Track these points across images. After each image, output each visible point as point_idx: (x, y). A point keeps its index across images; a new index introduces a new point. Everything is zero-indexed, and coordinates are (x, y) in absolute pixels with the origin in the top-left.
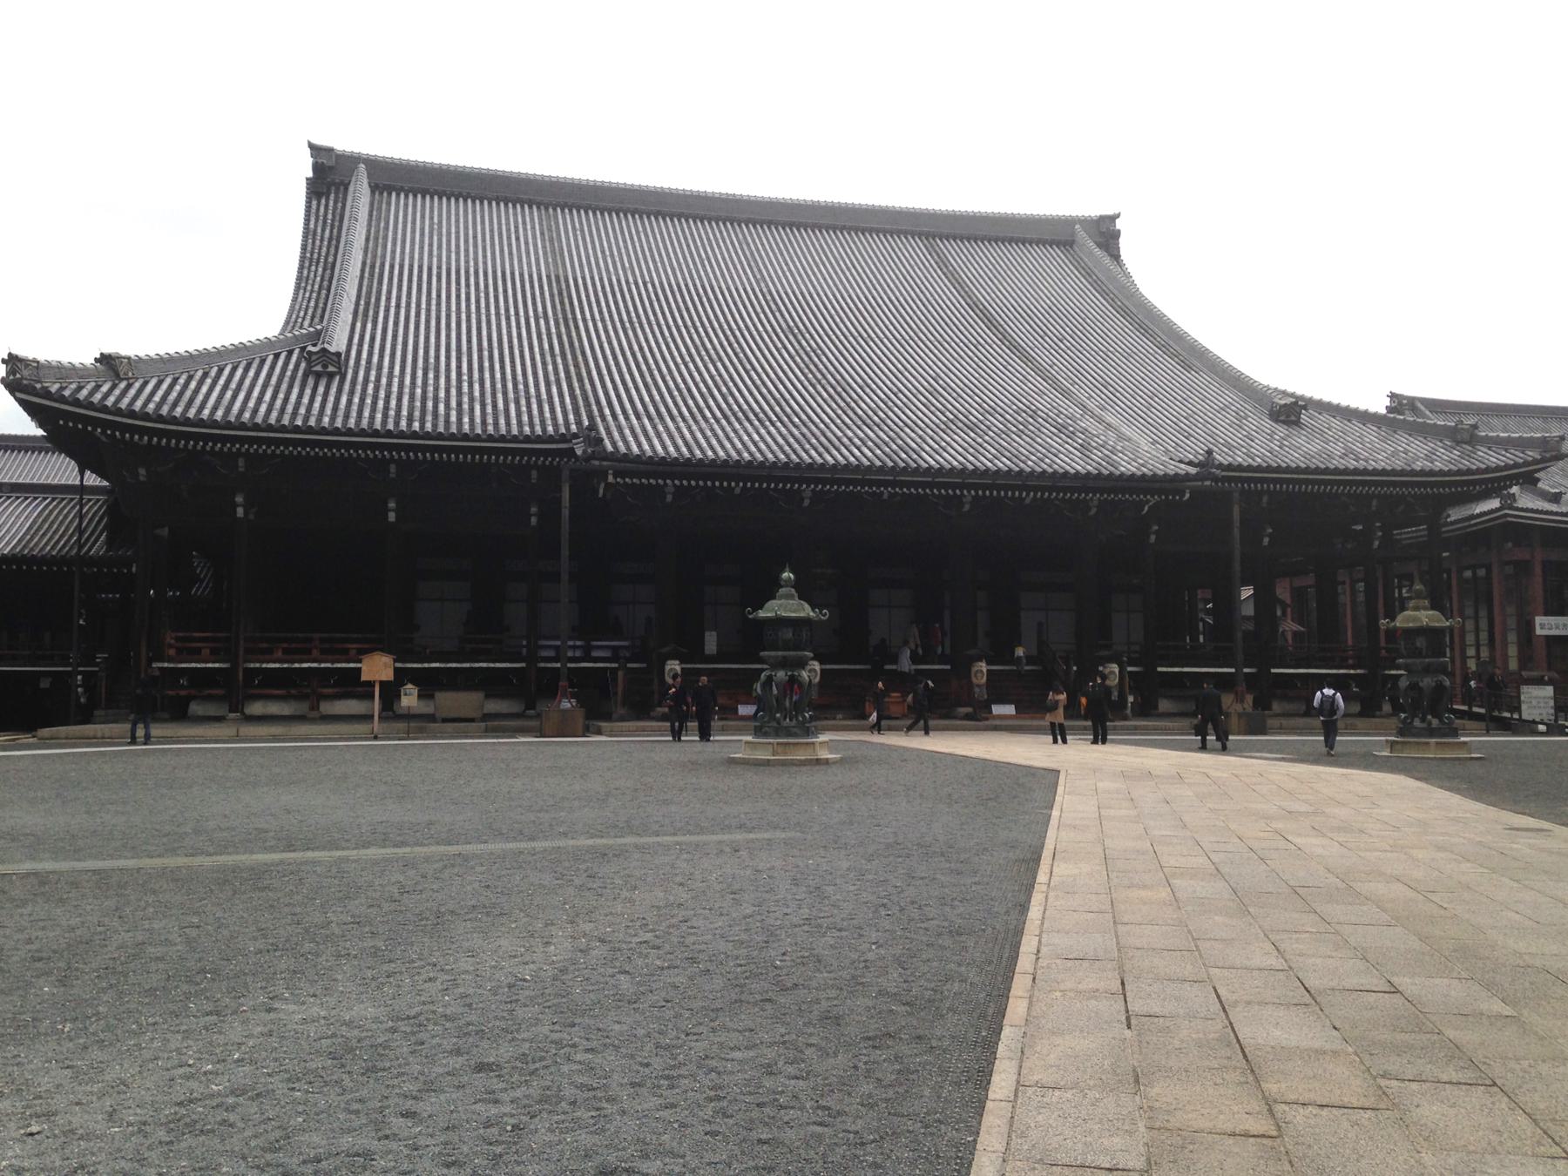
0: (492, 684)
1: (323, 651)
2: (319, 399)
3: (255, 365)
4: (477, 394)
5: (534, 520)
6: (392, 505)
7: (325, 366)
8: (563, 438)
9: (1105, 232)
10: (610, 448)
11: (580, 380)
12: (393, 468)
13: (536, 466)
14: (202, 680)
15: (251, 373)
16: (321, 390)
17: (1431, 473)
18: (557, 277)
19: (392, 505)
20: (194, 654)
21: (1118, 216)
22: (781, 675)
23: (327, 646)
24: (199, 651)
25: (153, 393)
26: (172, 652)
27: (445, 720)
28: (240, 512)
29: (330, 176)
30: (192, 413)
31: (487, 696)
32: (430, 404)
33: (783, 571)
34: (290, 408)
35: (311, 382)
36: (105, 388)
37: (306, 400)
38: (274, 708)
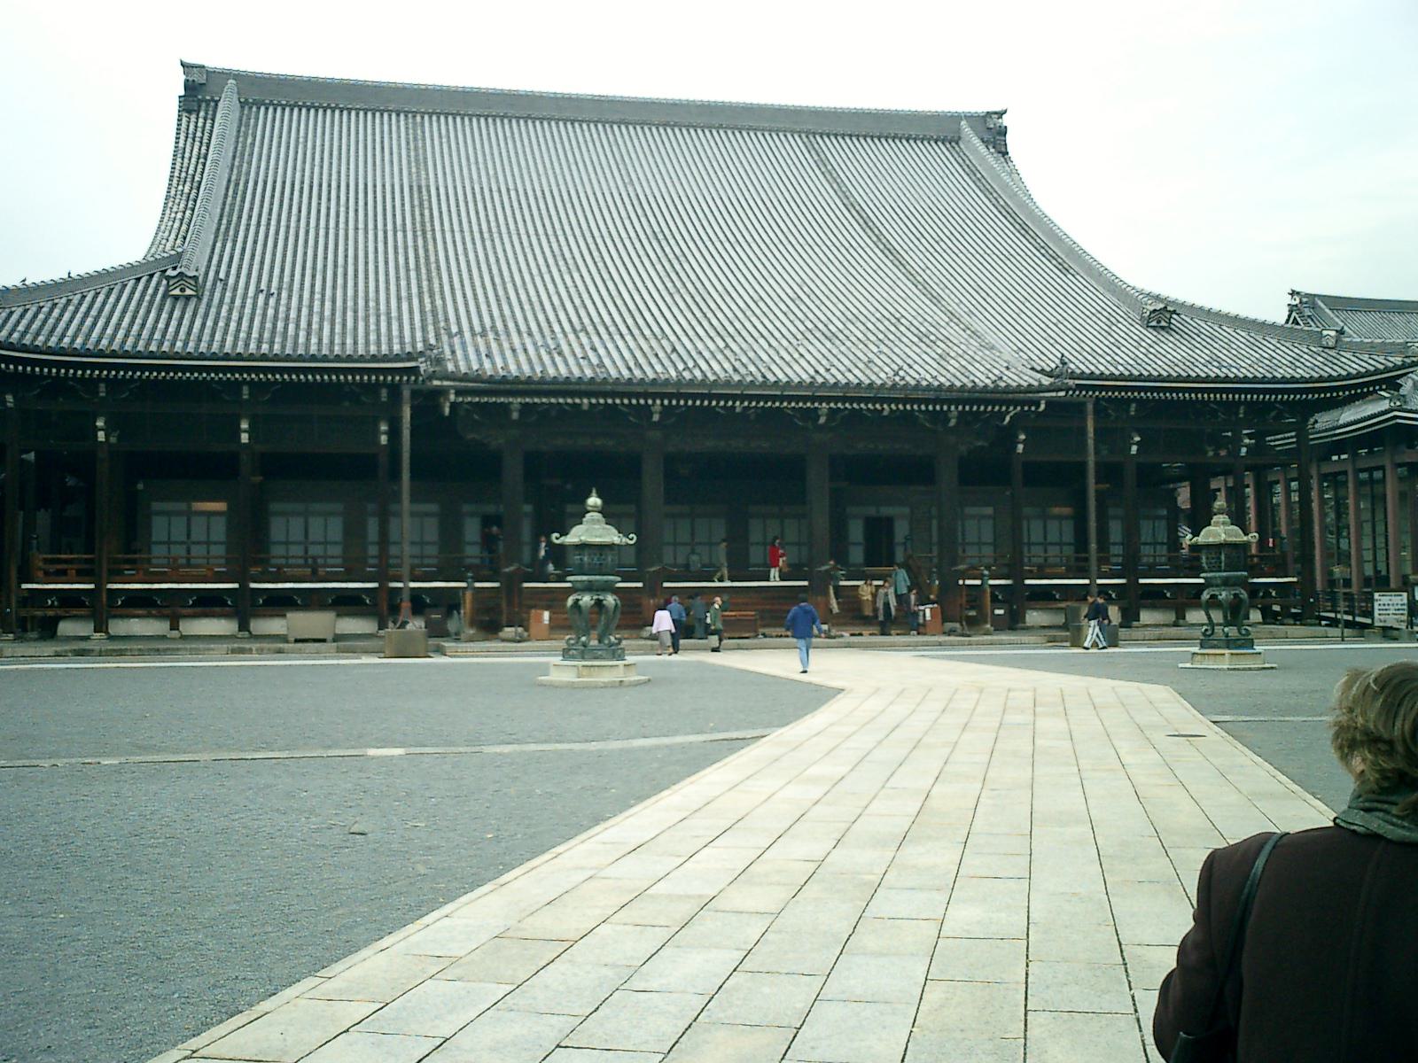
2: (174, 323)
3: (115, 292)
4: (327, 313)
6: (244, 425)
7: (182, 290)
8: (410, 357)
10: (450, 367)
11: (432, 296)
13: (385, 384)
14: (70, 602)
15: (112, 300)
16: (177, 314)
17: (1293, 380)
18: (420, 188)
19: (244, 425)
20: (60, 575)
22: (586, 600)
25: (18, 322)
26: (40, 574)
27: (297, 641)
28: (101, 436)
29: (200, 92)
30: (53, 342)
31: (338, 615)
32: (280, 325)
33: (589, 496)
34: (145, 334)
35: (168, 303)
37: (161, 325)
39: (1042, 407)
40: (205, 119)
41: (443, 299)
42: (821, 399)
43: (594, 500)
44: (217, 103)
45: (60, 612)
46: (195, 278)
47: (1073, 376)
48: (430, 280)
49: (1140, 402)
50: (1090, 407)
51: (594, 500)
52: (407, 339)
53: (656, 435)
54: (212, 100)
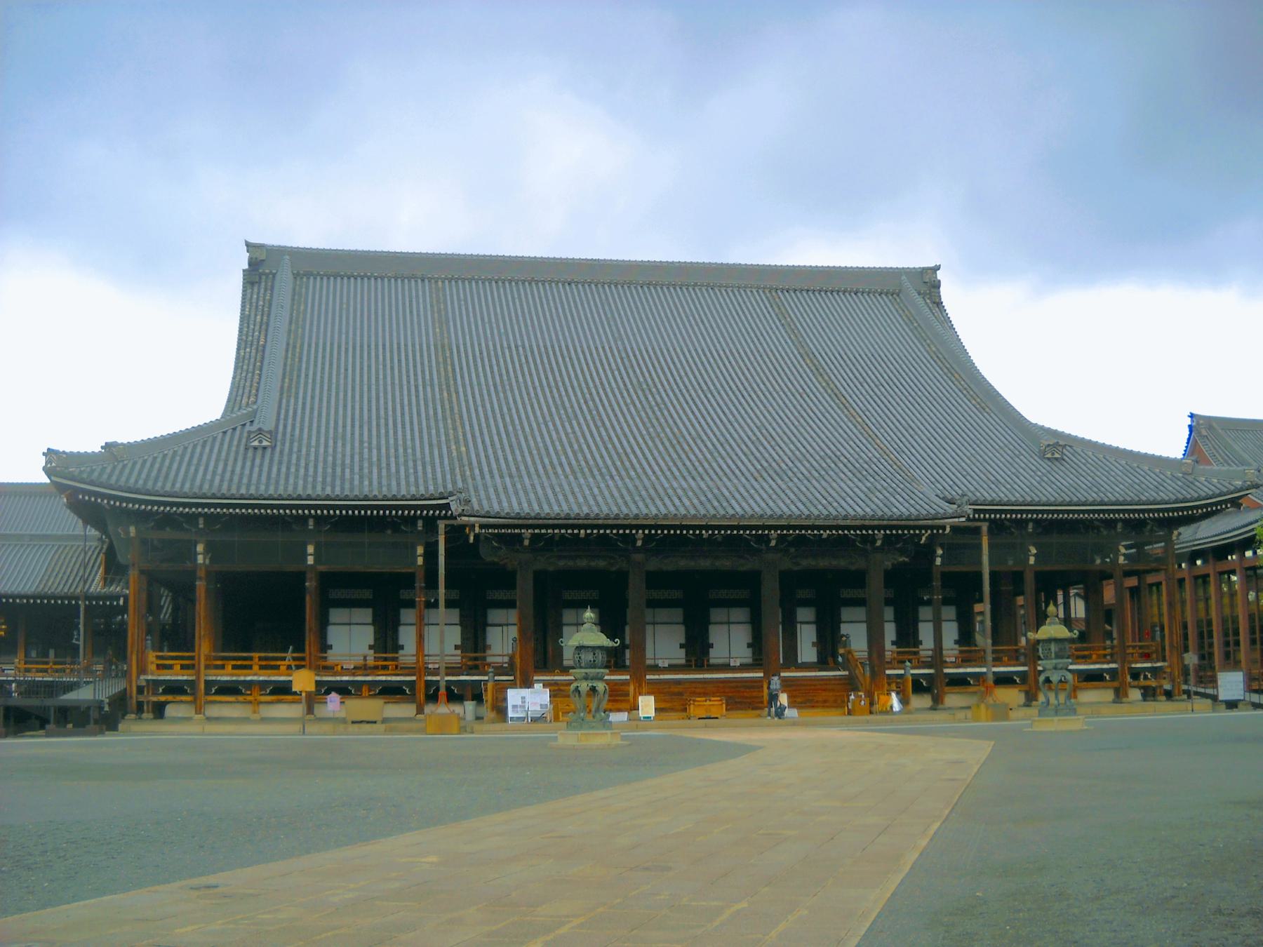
0: (390, 692)
1: (262, 667)
3: (209, 444)
4: (375, 459)
6: (310, 549)
7: (260, 442)
11: (457, 443)
12: (311, 522)
14: (175, 689)
15: (207, 450)
18: (443, 346)
19: (310, 549)
21: (938, 268)
23: (264, 663)
26: (153, 667)
32: (339, 470)
34: (236, 479)
35: (250, 454)
36: (108, 470)
37: (247, 472)
40: (266, 290)
41: (466, 446)
42: (770, 528)
44: (274, 275)
45: (170, 698)
46: (270, 432)
48: (455, 429)
49: (1037, 522)
52: (440, 481)
53: (638, 557)
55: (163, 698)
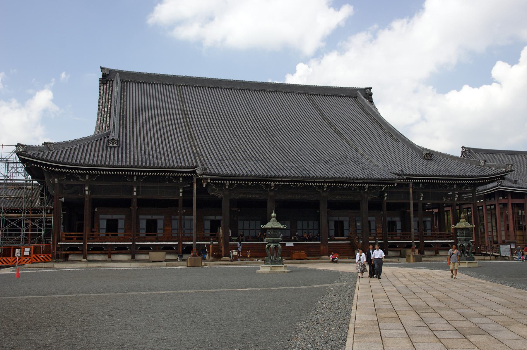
2: (112, 156)
5: (181, 194)
6: (135, 190)
7: (113, 144)
9: (367, 93)
14: (74, 248)
16: (112, 152)
20: (71, 239)
21: (371, 88)
22: (272, 245)
24: (72, 239)
25: (61, 155)
26: (64, 239)
27: (153, 262)
29: (107, 77)
33: (272, 213)
35: (109, 149)
36: (47, 154)
37: (108, 156)
38: (96, 257)
39: (396, 185)
40: (109, 87)
41: (199, 148)
43: (274, 214)
44: (113, 81)
45: (71, 252)
46: (117, 140)
47: (406, 175)
48: (193, 142)
49: (423, 183)
50: (411, 185)
51: (274, 214)
52: (190, 161)
53: (272, 194)
54: (111, 80)
55: (68, 252)
